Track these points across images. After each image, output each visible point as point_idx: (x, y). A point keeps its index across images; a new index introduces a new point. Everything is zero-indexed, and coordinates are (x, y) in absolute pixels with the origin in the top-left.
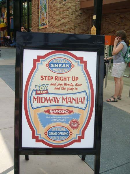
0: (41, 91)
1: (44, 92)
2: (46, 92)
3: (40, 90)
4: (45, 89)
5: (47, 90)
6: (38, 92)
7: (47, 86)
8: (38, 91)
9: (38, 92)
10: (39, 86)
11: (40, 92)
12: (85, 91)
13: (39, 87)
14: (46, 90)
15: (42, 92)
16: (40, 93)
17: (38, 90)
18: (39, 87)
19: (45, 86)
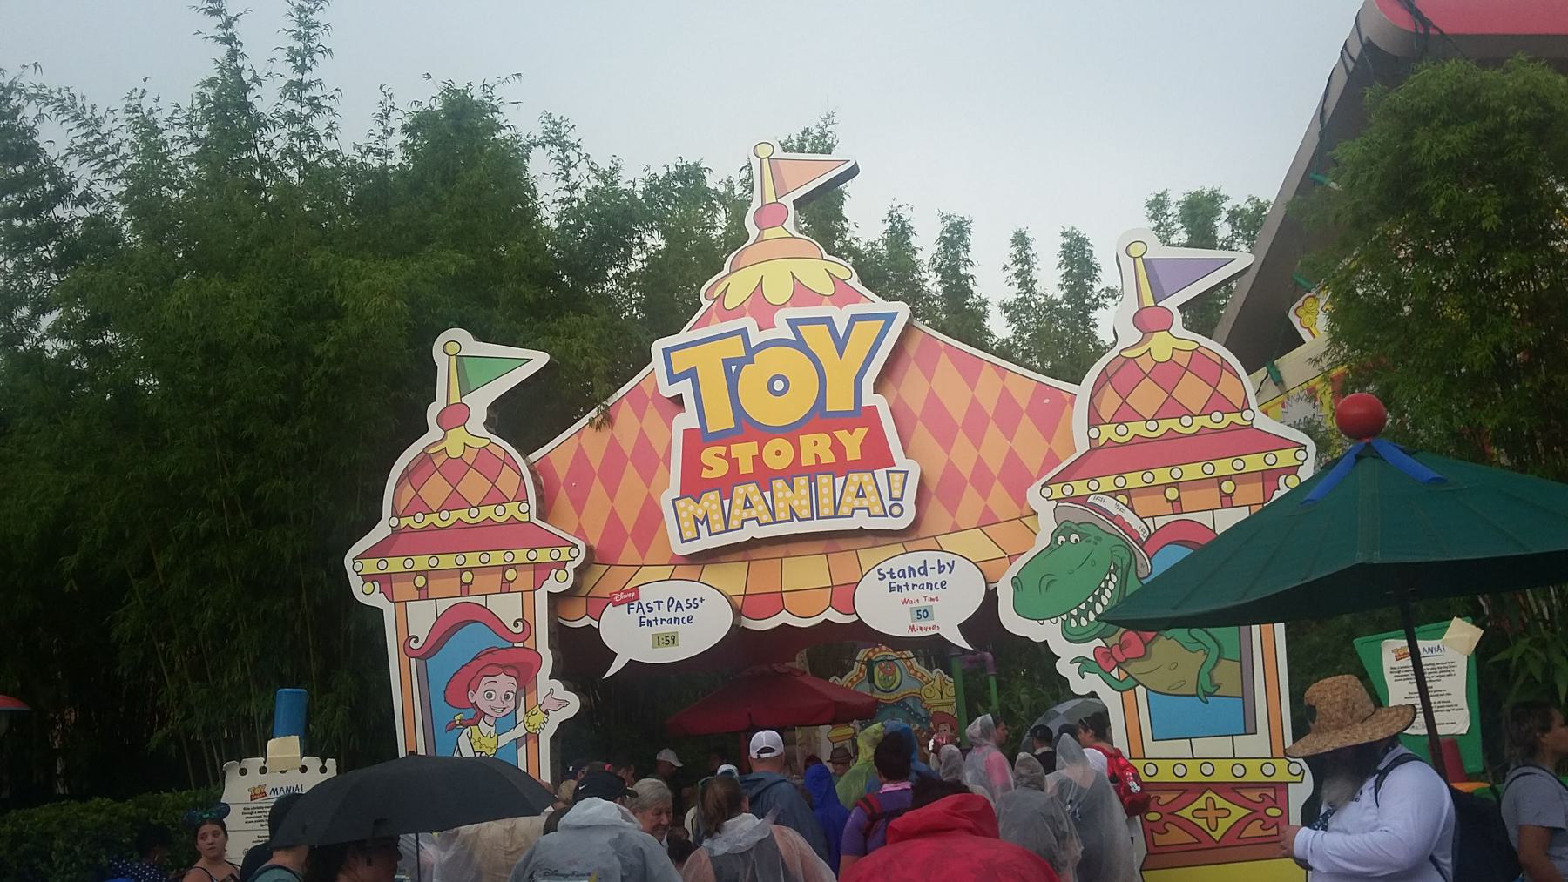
1: (816, 447)
2: (853, 442)
3: (747, 428)
4: (839, 400)
8: (724, 438)
9: (708, 455)
10: (735, 348)
11: (744, 453)
13: (732, 370)
15: (778, 454)
16: (746, 467)
18: (732, 370)
19: (841, 345)
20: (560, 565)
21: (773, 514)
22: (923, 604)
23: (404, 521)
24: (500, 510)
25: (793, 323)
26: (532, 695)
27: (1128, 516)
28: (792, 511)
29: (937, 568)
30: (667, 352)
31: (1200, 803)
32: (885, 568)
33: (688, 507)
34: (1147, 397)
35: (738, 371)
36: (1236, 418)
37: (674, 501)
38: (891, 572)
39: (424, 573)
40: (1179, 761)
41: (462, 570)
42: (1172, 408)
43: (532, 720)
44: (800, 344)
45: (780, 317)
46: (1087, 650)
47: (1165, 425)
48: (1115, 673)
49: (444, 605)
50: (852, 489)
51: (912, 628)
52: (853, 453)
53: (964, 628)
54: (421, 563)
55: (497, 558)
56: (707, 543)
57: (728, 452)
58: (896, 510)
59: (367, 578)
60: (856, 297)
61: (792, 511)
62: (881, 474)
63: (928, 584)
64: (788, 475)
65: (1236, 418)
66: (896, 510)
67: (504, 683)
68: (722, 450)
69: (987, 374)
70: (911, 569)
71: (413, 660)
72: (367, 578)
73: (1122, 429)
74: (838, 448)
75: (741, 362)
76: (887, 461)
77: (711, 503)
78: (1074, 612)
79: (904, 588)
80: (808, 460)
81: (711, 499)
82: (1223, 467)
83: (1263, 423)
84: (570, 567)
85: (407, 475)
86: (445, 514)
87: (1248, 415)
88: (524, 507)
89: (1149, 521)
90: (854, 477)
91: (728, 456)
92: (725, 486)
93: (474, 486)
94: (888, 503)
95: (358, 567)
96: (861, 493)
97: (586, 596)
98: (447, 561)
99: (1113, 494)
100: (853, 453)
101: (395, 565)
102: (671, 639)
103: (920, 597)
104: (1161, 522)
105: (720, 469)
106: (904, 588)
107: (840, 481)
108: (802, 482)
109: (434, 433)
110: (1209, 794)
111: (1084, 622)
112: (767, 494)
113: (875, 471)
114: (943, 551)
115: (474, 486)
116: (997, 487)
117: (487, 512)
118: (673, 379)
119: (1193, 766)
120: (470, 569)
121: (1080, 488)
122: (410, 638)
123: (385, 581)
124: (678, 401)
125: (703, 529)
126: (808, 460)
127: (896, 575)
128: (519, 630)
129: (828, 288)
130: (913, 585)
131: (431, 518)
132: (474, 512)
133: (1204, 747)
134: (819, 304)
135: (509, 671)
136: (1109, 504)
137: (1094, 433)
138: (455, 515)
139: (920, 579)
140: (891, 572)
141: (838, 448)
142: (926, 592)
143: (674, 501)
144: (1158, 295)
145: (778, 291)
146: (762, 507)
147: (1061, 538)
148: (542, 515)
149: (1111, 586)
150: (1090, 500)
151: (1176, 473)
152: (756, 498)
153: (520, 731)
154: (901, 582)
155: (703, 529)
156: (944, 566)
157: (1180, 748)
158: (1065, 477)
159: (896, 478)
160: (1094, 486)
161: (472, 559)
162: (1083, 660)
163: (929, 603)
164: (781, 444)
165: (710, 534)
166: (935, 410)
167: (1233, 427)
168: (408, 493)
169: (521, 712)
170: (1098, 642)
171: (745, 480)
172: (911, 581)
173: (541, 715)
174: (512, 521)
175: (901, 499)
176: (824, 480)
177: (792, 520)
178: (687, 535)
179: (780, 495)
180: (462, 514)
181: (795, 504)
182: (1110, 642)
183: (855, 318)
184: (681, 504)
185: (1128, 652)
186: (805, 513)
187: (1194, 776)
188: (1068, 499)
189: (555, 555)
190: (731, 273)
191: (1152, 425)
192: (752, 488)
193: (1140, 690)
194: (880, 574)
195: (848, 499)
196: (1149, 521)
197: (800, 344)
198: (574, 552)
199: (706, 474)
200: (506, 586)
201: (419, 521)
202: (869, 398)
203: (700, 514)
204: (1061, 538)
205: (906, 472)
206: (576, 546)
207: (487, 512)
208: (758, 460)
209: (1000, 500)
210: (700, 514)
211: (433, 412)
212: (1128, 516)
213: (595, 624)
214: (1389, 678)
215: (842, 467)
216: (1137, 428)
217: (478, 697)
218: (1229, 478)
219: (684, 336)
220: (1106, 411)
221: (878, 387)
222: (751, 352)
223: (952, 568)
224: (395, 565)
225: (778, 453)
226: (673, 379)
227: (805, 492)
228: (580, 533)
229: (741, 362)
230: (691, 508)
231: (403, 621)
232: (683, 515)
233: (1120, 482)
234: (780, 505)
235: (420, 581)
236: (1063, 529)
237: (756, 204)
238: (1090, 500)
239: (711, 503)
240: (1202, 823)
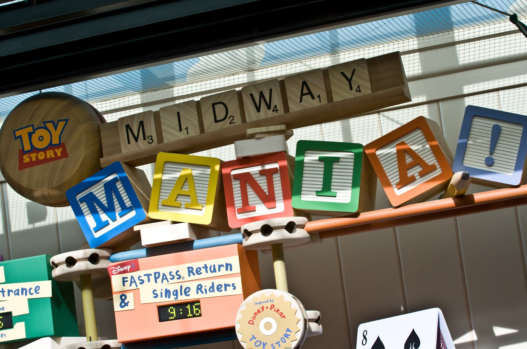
0: (38, 151)
1: (50, 154)
2: (59, 152)
3: (34, 149)
4: (56, 141)
5: (61, 145)
6: (26, 159)
7: (61, 125)
8: (29, 152)
9: (25, 157)
10: (30, 129)
11: (33, 156)
12: (216, 121)
13: (30, 135)
14: (57, 146)
15: (41, 156)
16: (34, 159)
17: (27, 147)
18: (30, 135)
19: (56, 128)
25: (44, 123)
44: (46, 128)
52: (59, 154)
68: (28, 155)
74: (55, 153)
80: (48, 157)
91: (29, 157)
100: (59, 154)
126: (48, 157)
141: (55, 153)
164: (42, 153)
197: (46, 128)
199: (25, 161)
208: (37, 157)
215: (56, 158)
225: (41, 155)
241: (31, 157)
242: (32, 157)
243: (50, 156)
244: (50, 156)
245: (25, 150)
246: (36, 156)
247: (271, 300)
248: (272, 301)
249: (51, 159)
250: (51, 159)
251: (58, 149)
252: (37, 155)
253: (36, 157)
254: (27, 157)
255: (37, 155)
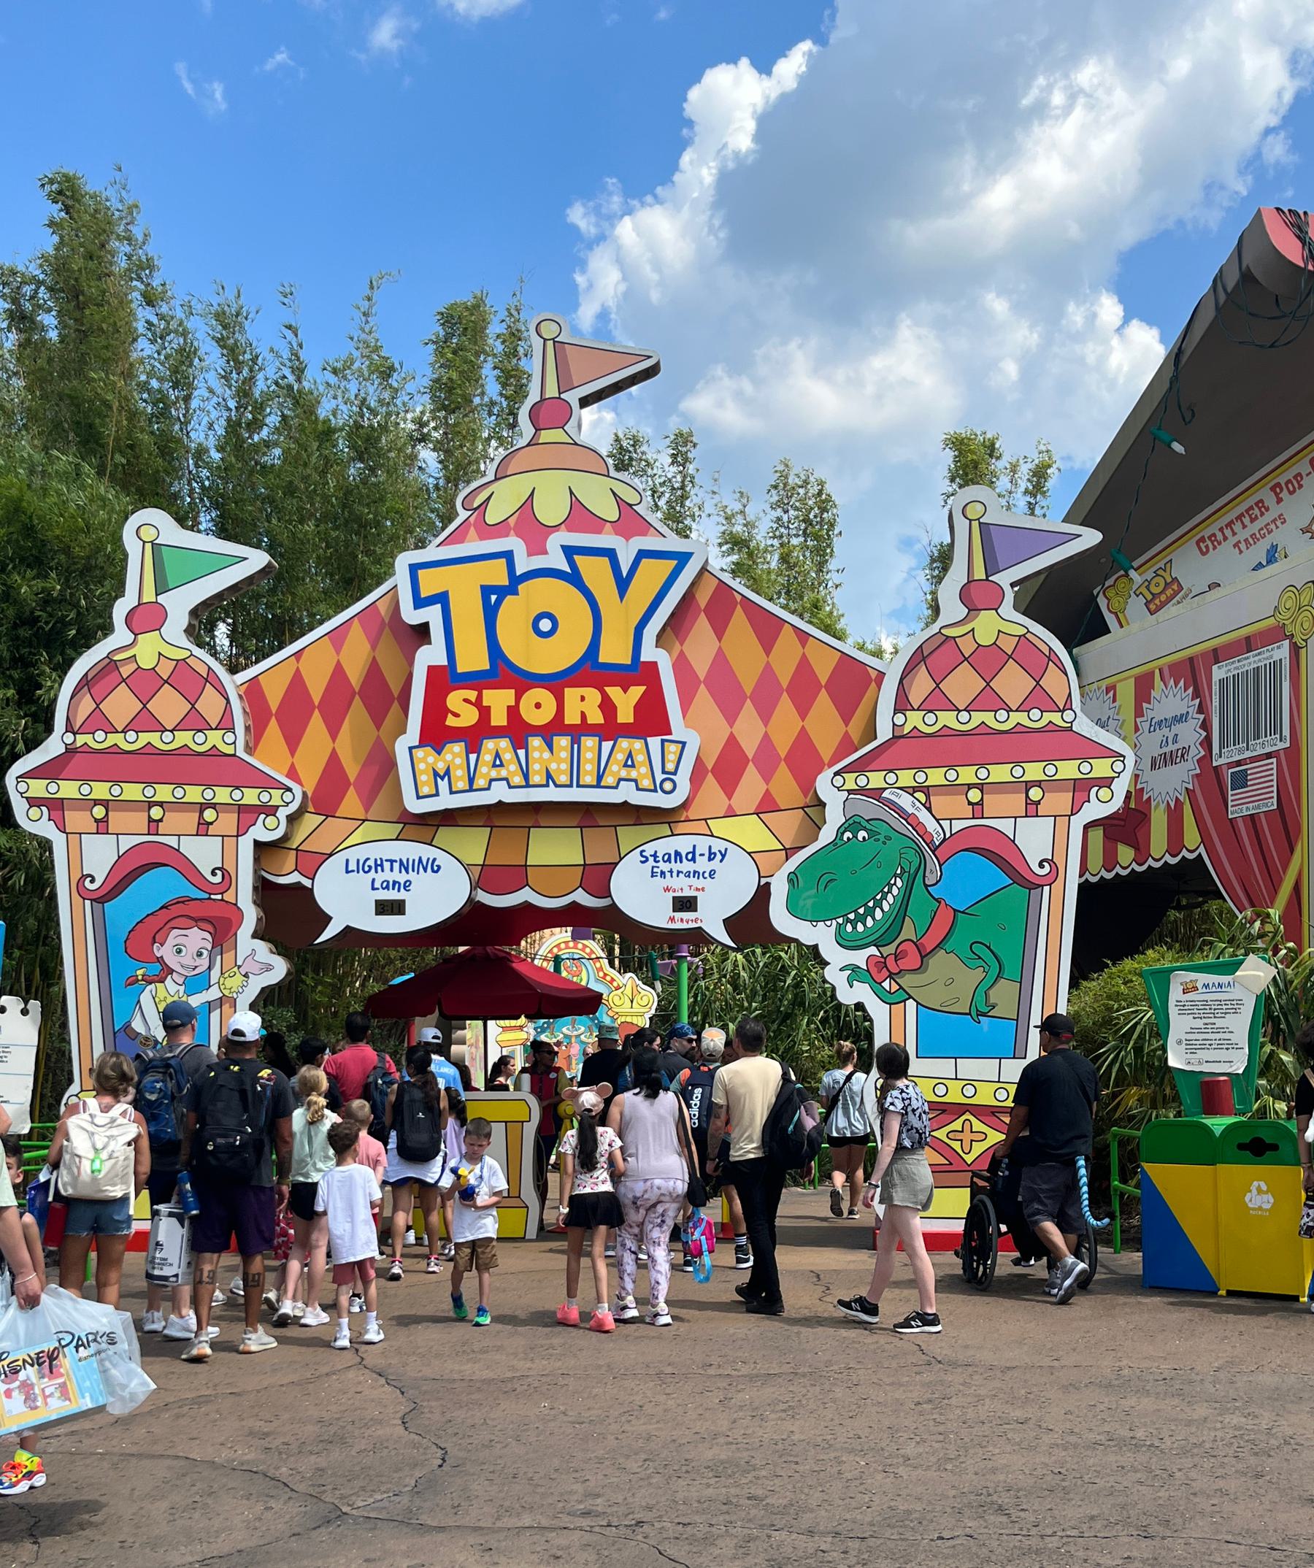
0: (521, 681)
2: (626, 702)
4: (614, 651)
8: (477, 681)
9: (455, 700)
10: (496, 574)
11: (499, 701)
13: (492, 599)
16: (499, 718)
18: (492, 599)
19: (623, 584)
20: (271, 811)
21: (526, 776)
22: (687, 893)
23: (81, 740)
24: (200, 737)
25: (569, 551)
26: (228, 956)
27: (924, 816)
28: (549, 776)
29: (707, 855)
30: (414, 569)
31: (957, 1125)
32: (649, 849)
33: (426, 757)
34: (963, 684)
35: (499, 602)
36: (1055, 718)
37: (411, 749)
38: (655, 856)
39: (105, 803)
40: (941, 1080)
41: (151, 805)
42: (988, 700)
43: (229, 982)
44: (574, 578)
45: (555, 542)
46: (860, 958)
47: (978, 718)
48: (886, 984)
49: (127, 843)
50: (620, 757)
51: (672, 919)
52: (625, 715)
53: (729, 923)
54: (101, 790)
55: (194, 794)
56: (446, 801)
57: (480, 697)
58: (668, 786)
59: (33, 802)
60: (643, 527)
61: (549, 776)
62: (654, 742)
63: (695, 872)
64: (550, 731)
65: (1055, 718)
66: (668, 786)
67: (197, 938)
68: (472, 695)
69: (786, 636)
70: (677, 854)
71: (88, 903)
72: (33, 802)
73: (930, 718)
74: (608, 707)
75: (503, 592)
76: (662, 727)
77: (455, 755)
78: (852, 916)
79: (668, 875)
80: (572, 718)
81: (455, 751)
82: (1034, 771)
83: (1085, 726)
84: (283, 813)
85: (86, 683)
86: (131, 736)
87: (1068, 715)
88: (229, 738)
89: (946, 824)
90: (624, 743)
91: (478, 703)
92: (473, 738)
93: (168, 705)
94: (659, 777)
95: (22, 787)
96: (629, 762)
97: (296, 849)
98: (133, 792)
99: (912, 791)
100: (625, 715)
101: (68, 789)
102: (396, 908)
103: (684, 887)
104: (958, 826)
105: (469, 717)
106: (668, 875)
107: (607, 745)
108: (563, 742)
109: (121, 635)
110: (967, 1116)
111: (860, 927)
112: (521, 753)
113: (649, 739)
114: (712, 836)
115: (168, 705)
116: (783, 772)
117: (183, 738)
118: (419, 603)
119: (955, 1087)
120: (161, 804)
121: (876, 780)
122: (84, 877)
123: (56, 807)
124: (422, 632)
125: (443, 785)
126: (572, 718)
127: (660, 859)
128: (218, 879)
129: (611, 513)
130: (679, 872)
131: (114, 739)
132: (167, 736)
133: (969, 1068)
134: (599, 531)
135: (200, 924)
136: (905, 801)
137: (899, 719)
138: (145, 738)
139: (687, 866)
140: (655, 856)
141: (608, 707)
142: (693, 881)
143: (411, 749)
144: (991, 568)
145: (551, 509)
146: (513, 767)
147: (848, 835)
148: (249, 750)
149: (895, 891)
150: (886, 794)
151: (983, 773)
152: (508, 756)
153: (213, 994)
154: (664, 866)
155: (443, 785)
156: (715, 854)
157: (944, 1067)
158: (859, 767)
159: (673, 749)
160: (891, 778)
161: (164, 792)
162: (854, 968)
163: (693, 893)
165: (452, 792)
166: (722, 673)
167: (1051, 728)
168: (86, 705)
169: (215, 973)
170: (873, 950)
171: (497, 732)
172: (676, 867)
173: (239, 978)
174: (214, 753)
175: (675, 773)
176: (589, 742)
177: (547, 785)
178: (425, 790)
179: (536, 755)
180: (154, 738)
181: (553, 767)
182: (886, 951)
183: (642, 554)
184: (419, 753)
185: (903, 964)
186: (564, 779)
187: (954, 1097)
188: (862, 791)
189: (265, 797)
190: (496, 479)
191: (964, 716)
192: (504, 744)
193: (911, 1004)
194: (642, 856)
195: (614, 767)
196: (946, 824)
197: (574, 578)
198: (288, 797)
199: (451, 721)
200: (203, 828)
201: (99, 740)
202: (649, 652)
203: (441, 768)
204: (848, 835)
205: (684, 744)
206: (289, 790)
207: (183, 738)
208: (513, 712)
209: (785, 785)
210: (441, 768)
211: (120, 610)
212: (924, 816)
213: (307, 883)
214: (1173, 1011)
215: (610, 730)
216: (947, 719)
217: (165, 951)
218: (1038, 784)
219: (432, 552)
220: (916, 697)
221: (660, 640)
222: (515, 581)
223: (723, 856)
224: (68, 789)
225: (538, 706)
226: (419, 603)
227: (565, 754)
228: (292, 774)
229: (503, 592)
230: (431, 760)
231: (75, 856)
232: (421, 766)
233: (921, 777)
234: (535, 767)
235: (99, 812)
236: (852, 824)
237: (534, 397)
238: (886, 794)
239: (455, 755)
240: (956, 1145)
241: (485, 703)
242: (489, 708)
243: (583, 716)
244: (583, 716)
245: (461, 669)
246: (513, 703)
247: (713, 851)
248: (719, 857)
249: (581, 730)
250: (581, 730)
251: (625, 691)
252: (518, 698)
253: (509, 708)
254: (466, 700)
255: (518, 698)
